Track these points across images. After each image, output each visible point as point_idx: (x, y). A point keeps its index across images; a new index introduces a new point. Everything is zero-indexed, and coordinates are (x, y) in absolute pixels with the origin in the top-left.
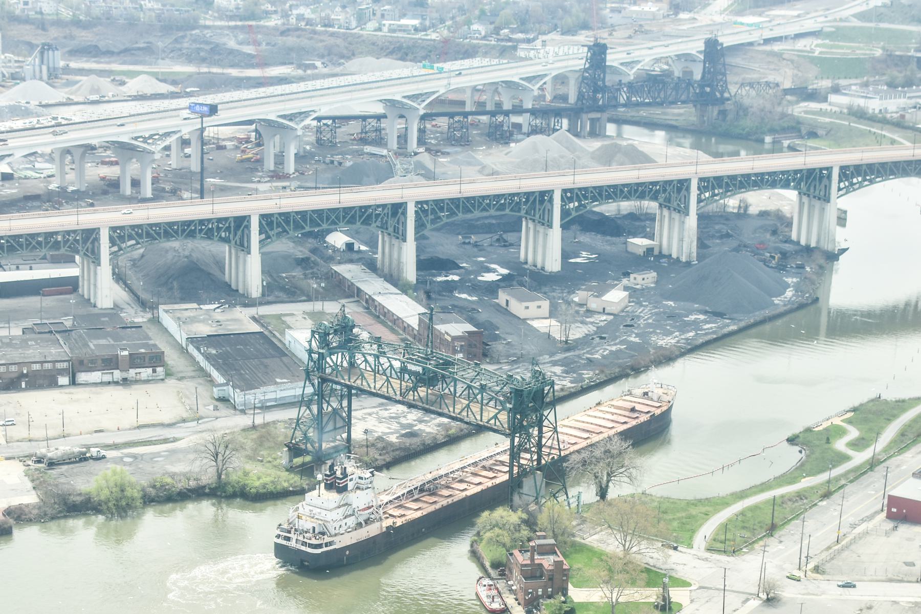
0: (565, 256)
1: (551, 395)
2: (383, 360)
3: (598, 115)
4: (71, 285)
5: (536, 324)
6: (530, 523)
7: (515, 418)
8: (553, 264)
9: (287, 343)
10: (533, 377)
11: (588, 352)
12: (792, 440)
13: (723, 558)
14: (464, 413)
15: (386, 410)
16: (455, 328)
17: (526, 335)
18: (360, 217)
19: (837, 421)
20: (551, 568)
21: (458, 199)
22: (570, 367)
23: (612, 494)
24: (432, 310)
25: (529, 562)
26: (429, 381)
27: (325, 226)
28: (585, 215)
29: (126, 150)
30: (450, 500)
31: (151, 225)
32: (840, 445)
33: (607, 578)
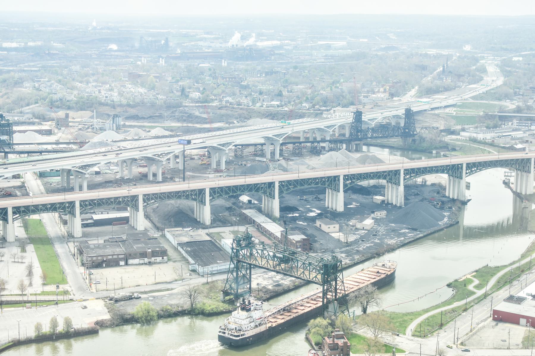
0: (346, 204)
1: (340, 266)
2: (265, 252)
3: (359, 142)
4: (126, 220)
5: (333, 235)
6: (332, 324)
7: (324, 277)
8: (340, 208)
9: (222, 245)
10: (332, 258)
11: (356, 247)
12: (449, 285)
13: (420, 339)
14: (302, 275)
16: (297, 237)
17: (329, 240)
18: (254, 188)
19: (469, 276)
20: (342, 345)
21: (298, 180)
22: (349, 254)
23: (369, 311)
24: (287, 229)
25: (332, 342)
26: (286, 260)
27: (239, 193)
28: (354, 186)
29: (150, 160)
31: (161, 193)
32: (471, 287)
33: (367, 349)
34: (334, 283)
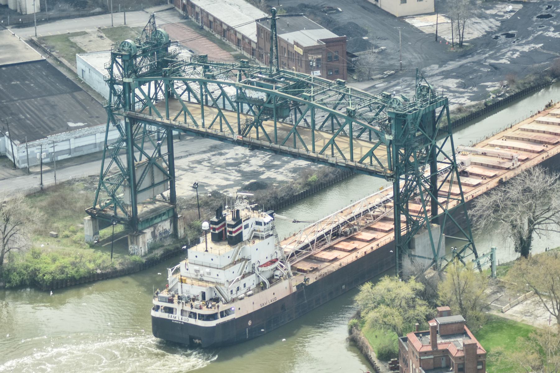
1: (444, 118)
2: (212, 87)
5: (417, 23)
6: (428, 295)
7: (397, 153)
9: (79, 73)
10: (419, 95)
11: (491, 57)
14: (328, 152)
15: (221, 154)
16: (307, 36)
17: (405, 39)
20: (460, 354)
22: (468, 79)
23: (538, 247)
24: (274, 13)
25: (429, 348)
30: (374, 245)
33: (537, 363)
34: (428, 168)
